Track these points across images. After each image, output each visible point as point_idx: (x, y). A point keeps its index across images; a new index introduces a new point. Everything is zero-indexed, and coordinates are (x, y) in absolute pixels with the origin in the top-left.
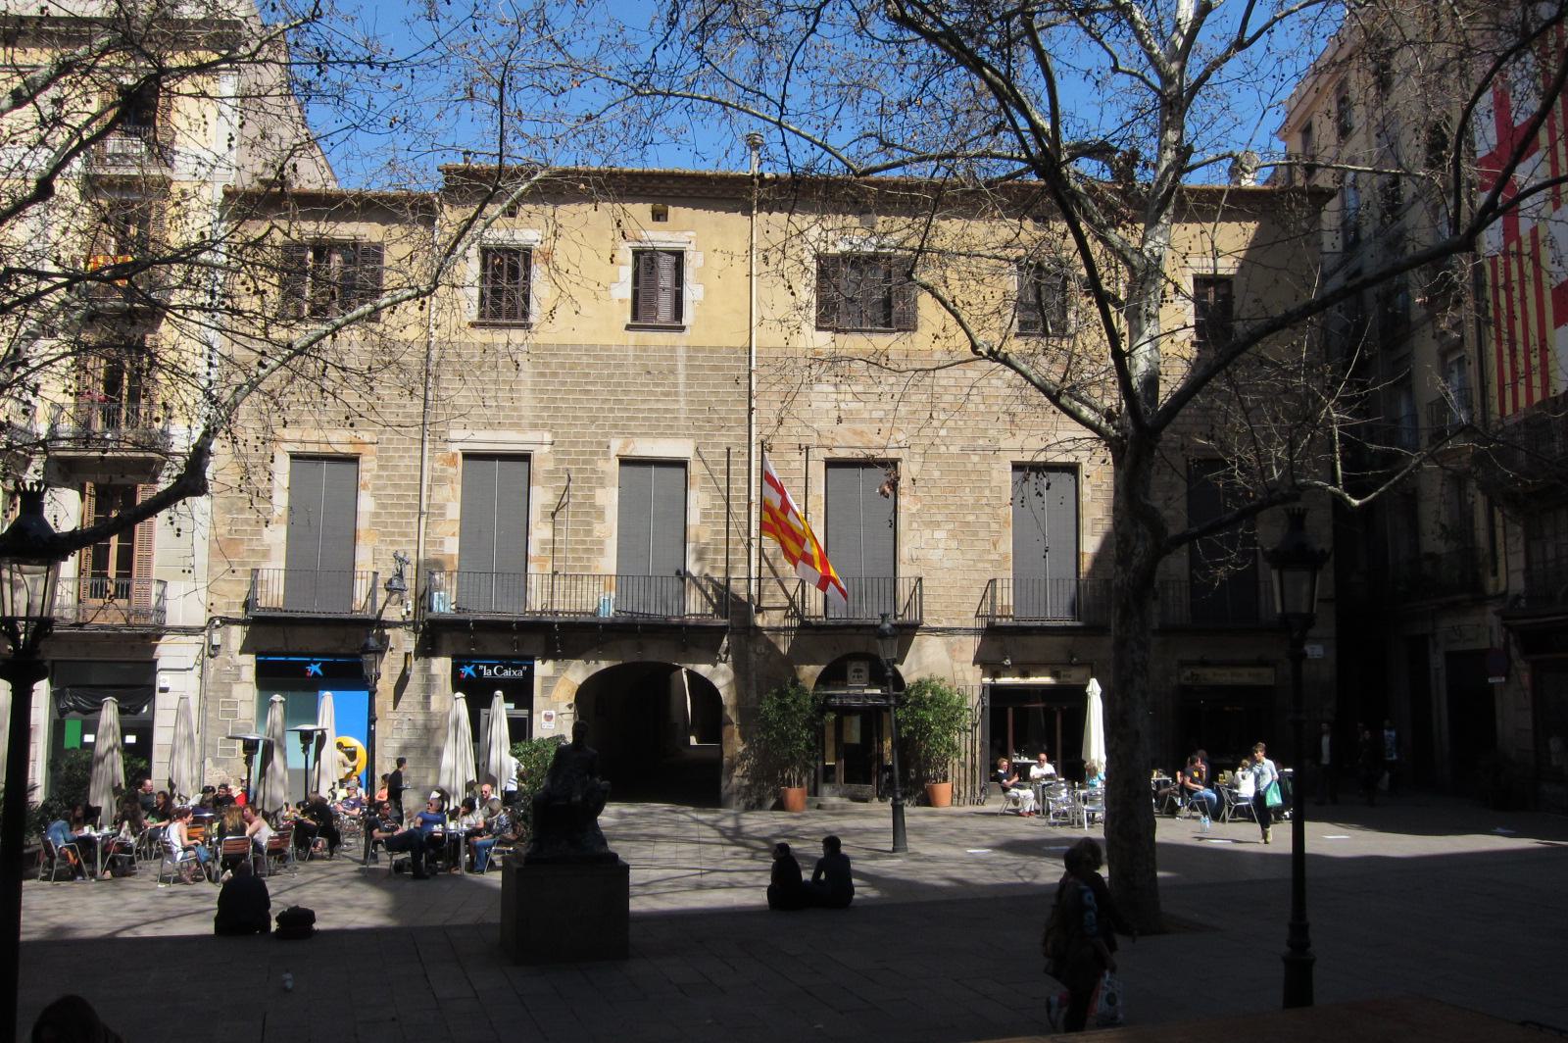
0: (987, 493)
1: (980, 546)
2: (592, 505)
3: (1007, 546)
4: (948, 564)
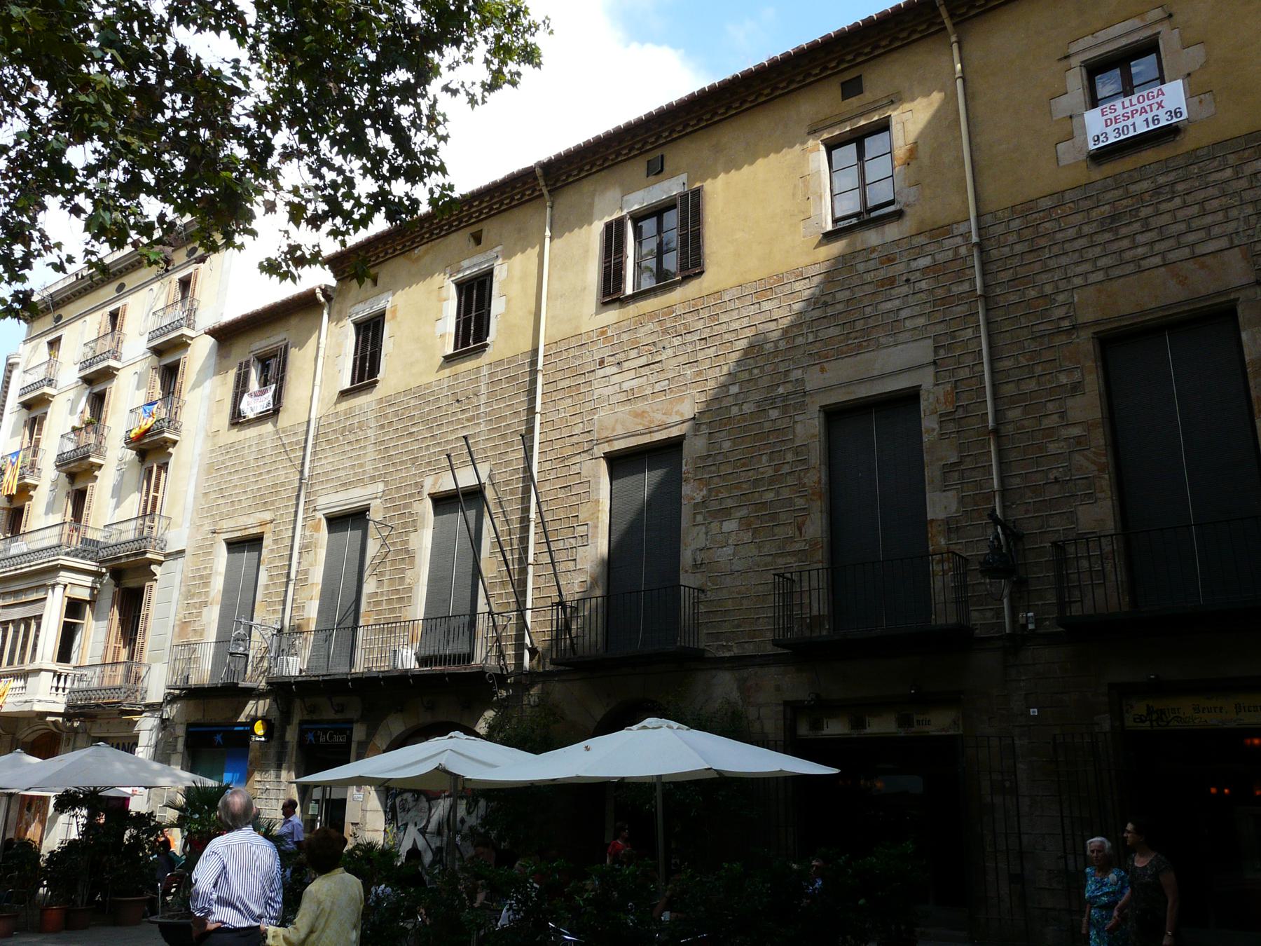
0: (790, 457)
1: (781, 533)
2: (407, 551)
3: (816, 527)
4: (738, 565)
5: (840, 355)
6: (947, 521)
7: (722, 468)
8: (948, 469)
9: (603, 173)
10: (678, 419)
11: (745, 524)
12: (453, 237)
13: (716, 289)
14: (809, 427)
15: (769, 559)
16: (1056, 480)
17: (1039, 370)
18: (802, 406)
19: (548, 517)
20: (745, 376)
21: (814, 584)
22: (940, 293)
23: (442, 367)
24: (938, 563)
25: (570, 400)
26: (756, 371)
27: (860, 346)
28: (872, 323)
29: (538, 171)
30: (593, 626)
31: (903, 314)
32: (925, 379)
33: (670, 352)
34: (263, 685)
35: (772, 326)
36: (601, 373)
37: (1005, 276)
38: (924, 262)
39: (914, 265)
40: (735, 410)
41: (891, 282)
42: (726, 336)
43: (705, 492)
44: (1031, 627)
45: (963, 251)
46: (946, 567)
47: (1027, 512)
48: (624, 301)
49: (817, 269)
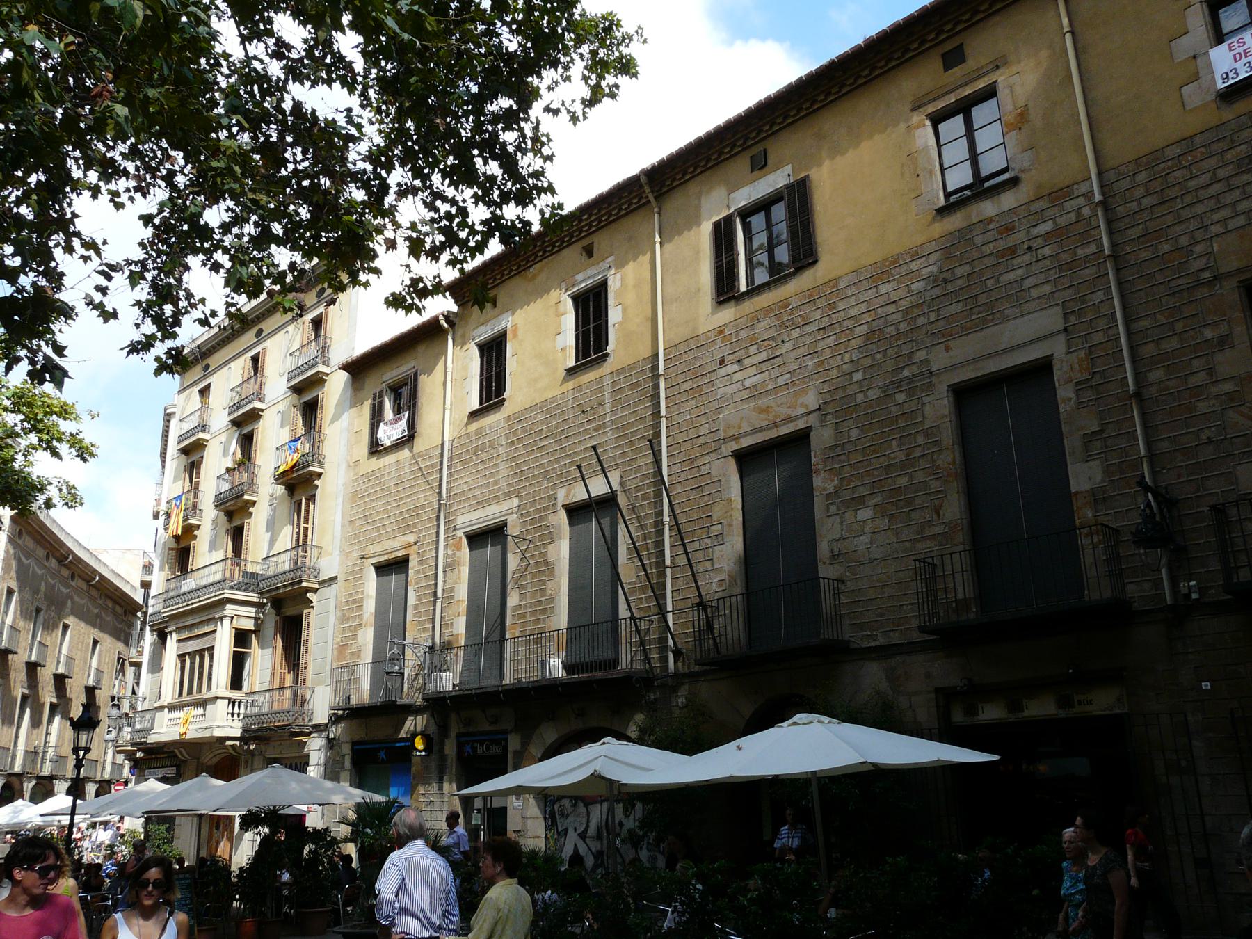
0: (920, 440)
2: (546, 563)
3: (954, 508)
5: (965, 331)
6: (1093, 492)
7: (851, 456)
8: (1088, 440)
9: (707, 174)
10: (803, 411)
11: (880, 510)
12: (565, 252)
13: (831, 277)
14: (939, 407)
15: (908, 544)
16: (1210, 441)
17: (1179, 327)
18: (929, 387)
19: (682, 520)
20: (868, 362)
21: (957, 567)
22: (1065, 257)
23: (565, 380)
24: (1087, 535)
25: (693, 402)
26: (878, 356)
27: (984, 320)
28: (995, 296)
29: (643, 178)
30: (735, 624)
31: (1027, 283)
32: (1057, 348)
33: (789, 345)
34: (419, 701)
35: (892, 308)
36: (722, 372)
37: (1134, 233)
38: (1047, 227)
39: (1035, 232)
40: (860, 397)
41: (1012, 251)
42: (845, 323)
43: (836, 482)
44: (1194, 596)
45: (1086, 211)
46: (1096, 540)
47: (1179, 476)
48: (739, 298)
49: (933, 247)
